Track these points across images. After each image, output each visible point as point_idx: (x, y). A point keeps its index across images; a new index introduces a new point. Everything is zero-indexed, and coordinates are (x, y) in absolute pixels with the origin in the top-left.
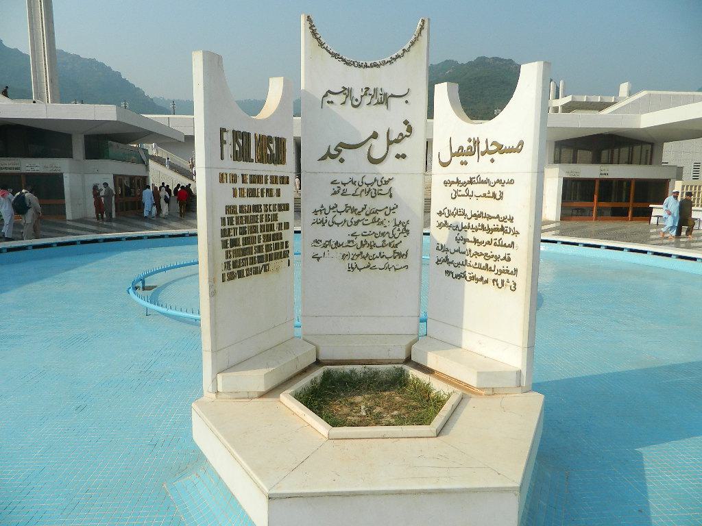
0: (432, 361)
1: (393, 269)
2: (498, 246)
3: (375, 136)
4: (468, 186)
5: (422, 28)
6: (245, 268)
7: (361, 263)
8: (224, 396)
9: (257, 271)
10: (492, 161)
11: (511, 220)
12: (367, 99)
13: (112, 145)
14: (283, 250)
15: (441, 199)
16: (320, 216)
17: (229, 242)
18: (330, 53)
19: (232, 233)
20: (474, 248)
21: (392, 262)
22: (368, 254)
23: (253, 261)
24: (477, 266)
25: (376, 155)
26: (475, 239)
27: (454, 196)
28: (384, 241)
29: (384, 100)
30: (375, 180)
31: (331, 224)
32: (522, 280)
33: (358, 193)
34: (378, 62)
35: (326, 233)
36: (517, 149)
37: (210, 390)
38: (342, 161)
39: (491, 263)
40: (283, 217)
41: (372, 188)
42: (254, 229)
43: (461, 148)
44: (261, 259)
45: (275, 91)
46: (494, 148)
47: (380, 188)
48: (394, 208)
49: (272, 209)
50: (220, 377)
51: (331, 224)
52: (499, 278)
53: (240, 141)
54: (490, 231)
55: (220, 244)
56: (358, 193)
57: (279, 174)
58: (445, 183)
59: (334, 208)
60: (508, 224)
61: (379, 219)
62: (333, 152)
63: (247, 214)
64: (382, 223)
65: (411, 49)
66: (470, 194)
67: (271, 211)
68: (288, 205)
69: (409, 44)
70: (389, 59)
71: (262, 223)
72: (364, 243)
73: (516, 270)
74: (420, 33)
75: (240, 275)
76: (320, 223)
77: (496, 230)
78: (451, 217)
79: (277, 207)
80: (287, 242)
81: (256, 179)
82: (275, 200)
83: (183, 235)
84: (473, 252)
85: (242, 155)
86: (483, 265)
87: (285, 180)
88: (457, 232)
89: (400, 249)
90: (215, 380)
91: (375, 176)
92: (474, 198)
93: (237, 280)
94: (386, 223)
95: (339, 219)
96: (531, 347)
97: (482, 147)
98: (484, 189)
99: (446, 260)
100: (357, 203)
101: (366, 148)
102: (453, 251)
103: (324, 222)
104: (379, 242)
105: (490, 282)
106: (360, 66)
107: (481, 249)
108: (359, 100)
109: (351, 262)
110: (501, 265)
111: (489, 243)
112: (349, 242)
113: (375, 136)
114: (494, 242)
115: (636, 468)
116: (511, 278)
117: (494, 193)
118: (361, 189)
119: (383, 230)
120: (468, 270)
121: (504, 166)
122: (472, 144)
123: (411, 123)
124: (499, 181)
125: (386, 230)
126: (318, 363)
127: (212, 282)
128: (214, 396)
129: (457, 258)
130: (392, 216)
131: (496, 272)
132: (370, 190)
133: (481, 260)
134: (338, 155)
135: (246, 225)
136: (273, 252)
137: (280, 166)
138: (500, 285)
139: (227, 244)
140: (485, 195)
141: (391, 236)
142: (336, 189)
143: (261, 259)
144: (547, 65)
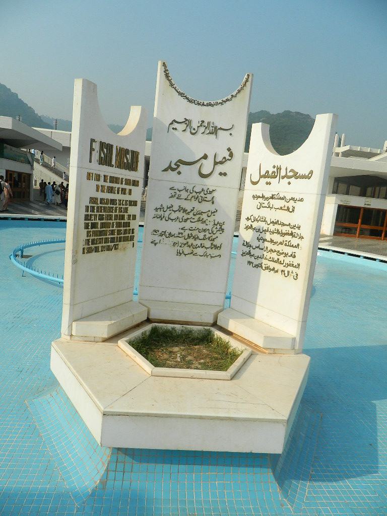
0: (232, 326)
1: (209, 257)
2: (288, 246)
3: (205, 157)
5: (247, 81)
6: (100, 245)
7: (187, 250)
8: (76, 338)
9: (109, 249)
10: (289, 183)
11: (299, 228)
12: (202, 129)
13: (6, 147)
14: (129, 235)
15: (249, 208)
16: (160, 213)
17: (90, 224)
18: (177, 92)
19: (93, 218)
20: (270, 246)
21: (209, 251)
23: (106, 241)
24: (271, 259)
25: (205, 171)
26: (271, 239)
28: (205, 235)
29: (215, 131)
30: (203, 190)
31: (167, 219)
32: (303, 272)
33: (189, 198)
34: (212, 103)
35: (162, 226)
37: (67, 333)
38: (179, 173)
39: (281, 258)
40: (133, 210)
42: (110, 217)
43: (268, 172)
44: (113, 240)
45: (135, 114)
46: (291, 174)
47: (205, 196)
48: (214, 212)
49: (124, 204)
50: (74, 324)
51: (167, 219)
52: (286, 270)
53: (105, 150)
55: (83, 226)
57: (132, 179)
58: (254, 197)
60: (296, 231)
61: (203, 219)
63: (105, 206)
64: (205, 222)
66: (271, 206)
67: (123, 205)
68: (138, 182)
69: (237, 91)
70: (220, 101)
72: (190, 235)
73: (299, 265)
74: (245, 85)
75: (97, 250)
76: (159, 218)
78: (256, 222)
79: (128, 202)
80: (133, 230)
81: (114, 180)
82: (127, 197)
83: (55, 220)
84: (269, 249)
85: (105, 161)
86: (276, 259)
87: (135, 183)
88: (259, 233)
90: (70, 326)
91: (203, 187)
92: (273, 210)
93: (94, 254)
94: (207, 222)
95: (173, 216)
97: (283, 173)
98: (281, 203)
99: (249, 253)
100: (188, 206)
101: (198, 165)
102: (254, 247)
103: (162, 217)
104: (201, 235)
105: (280, 272)
106: (199, 104)
108: (196, 128)
110: (288, 260)
111: (281, 243)
113: (205, 157)
114: (285, 243)
115: (371, 415)
116: (295, 270)
117: (288, 207)
118: (191, 195)
119: (204, 227)
120: (264, 262)
121: (297, 188)
123: (233, 150)
124: (292, 199)
125: (207, 227)
126: (148, 321)
127: (75, 253)
128: (69, 338)
129: (257, 252)
131: (284, 265)
132: (198, 197)
134: (176, 169)
135: (104, 214)
136: (122, 235)
137: (133, 173)
138: (286, 275)
139: (88, 226)
141: (210, 232)
142: (173, 194)
143: (113, 240)
144: (335, 117)
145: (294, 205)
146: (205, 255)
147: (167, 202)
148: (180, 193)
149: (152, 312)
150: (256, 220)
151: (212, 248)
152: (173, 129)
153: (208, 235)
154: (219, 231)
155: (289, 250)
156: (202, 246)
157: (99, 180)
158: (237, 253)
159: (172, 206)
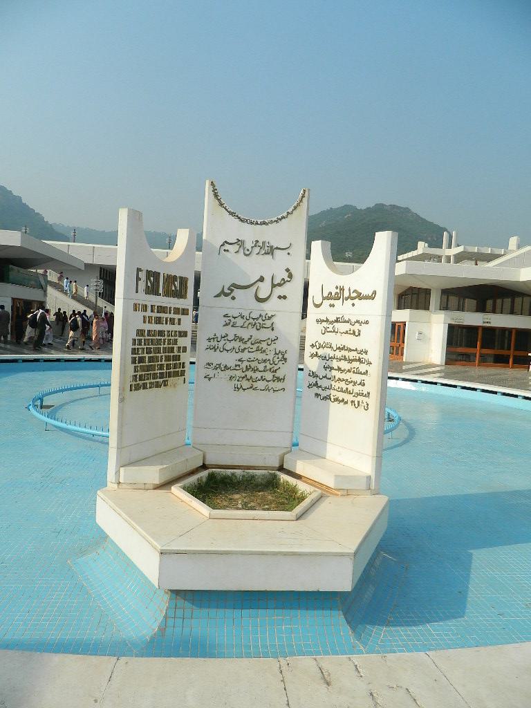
0: (300, 467)
1: (272, 391)
2: (356, 373)
3: (262, 279)
4: (335, 324)
5: (303, 197)
6: (148, 381)
7: (245, 384)
8: (124, 486)
9: (158, 385)
10: (353, 305)
11: (366, 352)
12: (257, 250)
13: (12, 269)
14: (180, 370)
15: (313, 333)
16: (213, 343)
19: (140, 352)
20: (338, 375)
21: (271, 385)
22: (251, 377)
23: (155, 376)
25: (262, 295)
26: (338, 367)
27: (323, 332)
29: (271, 251)
30: (260, 316)
31: (221, 350)
32: (373, 401)
33: (246, 325)
35: (217, 358)
36: (372, 297)
38: (233, 298)
39: (350, 387)
40: (182, 342)
41: (257, 322)
44: (162, 375)
45: (183, 238)
46: (354, 295)
50: (122, 470)
51: (221, 350)
53: (152, 279)
54: (350, 361)
56: (246, 325)
57: (181, 307)
58: (317, 321)
59: (225, 337)
60: (364, 356)
62: (226, 291)
63: (153, 338)
64: (264, 351)
65: (294, 212)
71: (165, 346)
73: (369, 393)
74: (301, 201)
75: (145, 387)
77: (355, 360)
81: (162, 309)
82: (176, 328)
85: (152, 290)
86: (344, 389)
87: (185, 312)
89: (279, 374)
90: (118, 473)
92: (339, 334)
96: (379, 458)
97: (346, 294)
101: (254, 289)
102: (321, 377)
104: (261, 367)
105: (349, 402)
106: (252, 223)
107: (343, 376)
109: (236, 382)
110: (357, 389)
111: (349, 371)
112: (236, 366)
113: (262, 279)
115: (465, 565)
116: (365, 399)
118: (248, 322)
120: (333, 393)
122: (338, 291)
123: (292, 271)
124: (358, 322)
125: (268, 357)
126: (204, 467)
127: (122, 390)
128: (116, 486)
129: (324, 383)
130: (273, 346)
132: (255, 324)
133: (343, 385)
134: (230, 294)
135: (152, 346)
136: (172, 370)
138: (356, 406)
140: (347, 333)
141: (272, 362)
142: (228, 322)
143: (162, 375)
145: (360, 328)
146: (267, 389)
147: (222, 331)
148: (235, 320)
149: (208, 457)
150: (321, 346)
151: (274, 381)
152: (225, 250)
153: (269, 366)
154: (281, 360)
155: (358, 378)
156: (263, 379)
157: (146, 311)
158: (302, 388)
159: (227, 335)
